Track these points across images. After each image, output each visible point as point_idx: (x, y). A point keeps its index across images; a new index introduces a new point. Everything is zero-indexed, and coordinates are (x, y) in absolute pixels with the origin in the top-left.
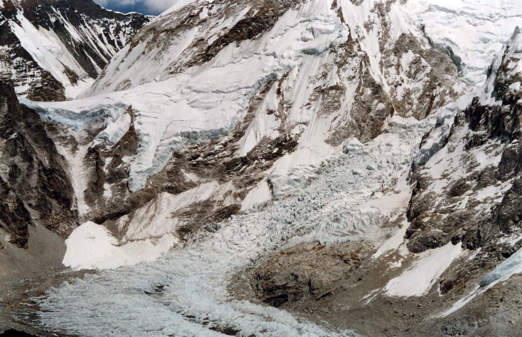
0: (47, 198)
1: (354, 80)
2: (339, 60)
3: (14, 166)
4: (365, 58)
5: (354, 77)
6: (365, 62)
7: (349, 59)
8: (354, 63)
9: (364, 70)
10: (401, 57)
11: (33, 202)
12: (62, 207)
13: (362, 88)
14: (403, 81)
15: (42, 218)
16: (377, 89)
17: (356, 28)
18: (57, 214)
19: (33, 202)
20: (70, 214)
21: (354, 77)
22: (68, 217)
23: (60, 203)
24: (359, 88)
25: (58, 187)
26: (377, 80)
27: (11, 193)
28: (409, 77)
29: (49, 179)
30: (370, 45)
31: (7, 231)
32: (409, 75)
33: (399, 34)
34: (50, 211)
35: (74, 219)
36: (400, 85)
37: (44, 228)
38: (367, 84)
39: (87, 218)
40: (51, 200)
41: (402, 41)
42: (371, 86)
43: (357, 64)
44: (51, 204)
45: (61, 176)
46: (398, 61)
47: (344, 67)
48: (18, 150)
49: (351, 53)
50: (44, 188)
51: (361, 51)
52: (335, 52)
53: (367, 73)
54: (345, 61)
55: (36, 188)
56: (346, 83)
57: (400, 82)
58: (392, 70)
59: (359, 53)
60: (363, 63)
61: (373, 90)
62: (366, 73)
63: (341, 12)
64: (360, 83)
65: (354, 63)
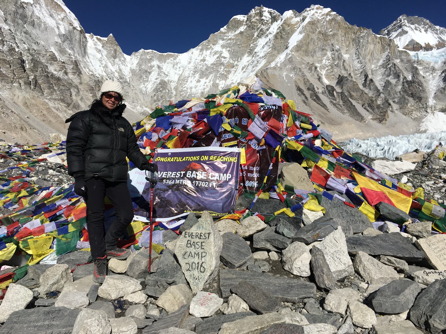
0: (406, 97)
3: (388, 81)
11: (396, 100)
12: (415, 102)
15: (400, 109)
18: (412, 106)
19: (396, 100)
20: (421, 106)
22: (420, 108)
23: (414, 99)
25: (415, 91)
27: (382, 95)
29: (409, 87)
31: (371, 113)
34: (407, 104)
35: (425, 108)
37: (401, 114)
39: (434, 109)
40: (408, 98)
44: (408, 100)
45: (419, 85)
48: (392, 72)
50: (405, 91)
55: (400, 92)
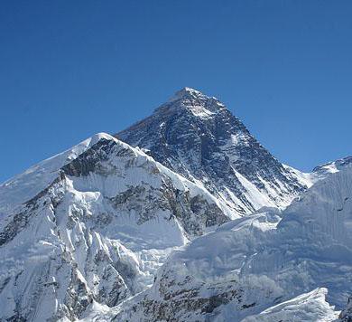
16: (82, 286)
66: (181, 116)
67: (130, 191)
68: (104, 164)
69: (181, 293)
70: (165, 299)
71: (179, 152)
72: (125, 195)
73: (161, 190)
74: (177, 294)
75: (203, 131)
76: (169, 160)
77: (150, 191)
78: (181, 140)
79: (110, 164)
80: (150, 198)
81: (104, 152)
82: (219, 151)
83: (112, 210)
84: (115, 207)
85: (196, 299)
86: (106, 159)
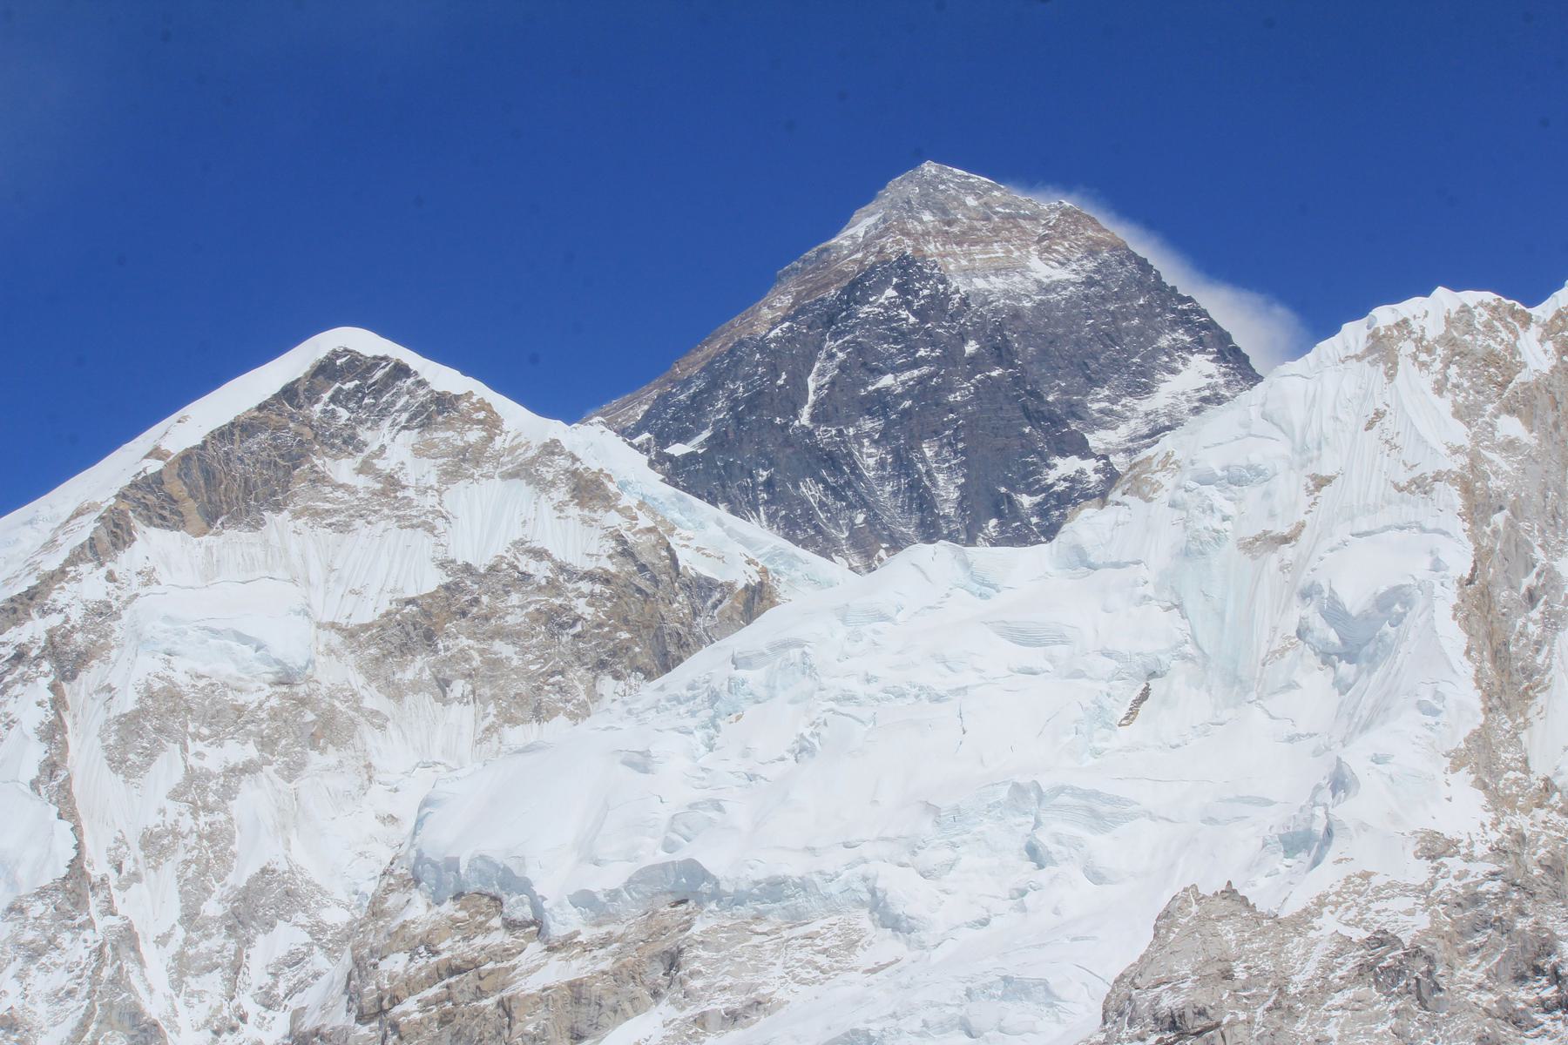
1: (71, 1004)
2: (29, 935)
4: (128, 938)
5: (70, 993)
6: (114, 948)
7: (65, 938)
8: (77, 949)
9: (107, 972)
10: (249, 942)
13: (93, 1027)
14: (243, 1018)
17: (113, 845)
21: (70, 993)
24: (83, 1027)
26: (154, 1009)
28: (269, 1007)
30: (151, 905)
32: (269, 1001)
33: (252, 869)
36: (233, 1029)
38: (114, 1017)
41: (262, 892)
42: (127, 1024)
43: (85, 953)
46: (238, 953)
47: (44, 959)
49: (73, 918)
51: (113, 914)
52: (22, 911)
53: (118, 981)
54: (50, 942)
56: (42, 1010)
57: (235, 1021)
58: (214, 983)
59: (102, 923)
60: (108, 949)
61: (132, 1037)
62: (112, 981)
63: (69, 792)
64: (89, 1014)
65: (77, 949)
66: (879, 288)
67: (451, 589)
68: (343, 469)
69: (430, 981)
70: (362, 1018)
71: (869, 458)
72: (427, 614)
73: (607, 580)
74: (412, 986)
75: (1000, 353)
76: (811, 491)
77: (552, 587)
78: (879, 404)
79: (365, 468)
80: (556, 620)
81: (343, 414)
82: (1083, 451)
83: (358, 680)
84: (375, 670)
85: (489, 1002)
86: (351, 443)
